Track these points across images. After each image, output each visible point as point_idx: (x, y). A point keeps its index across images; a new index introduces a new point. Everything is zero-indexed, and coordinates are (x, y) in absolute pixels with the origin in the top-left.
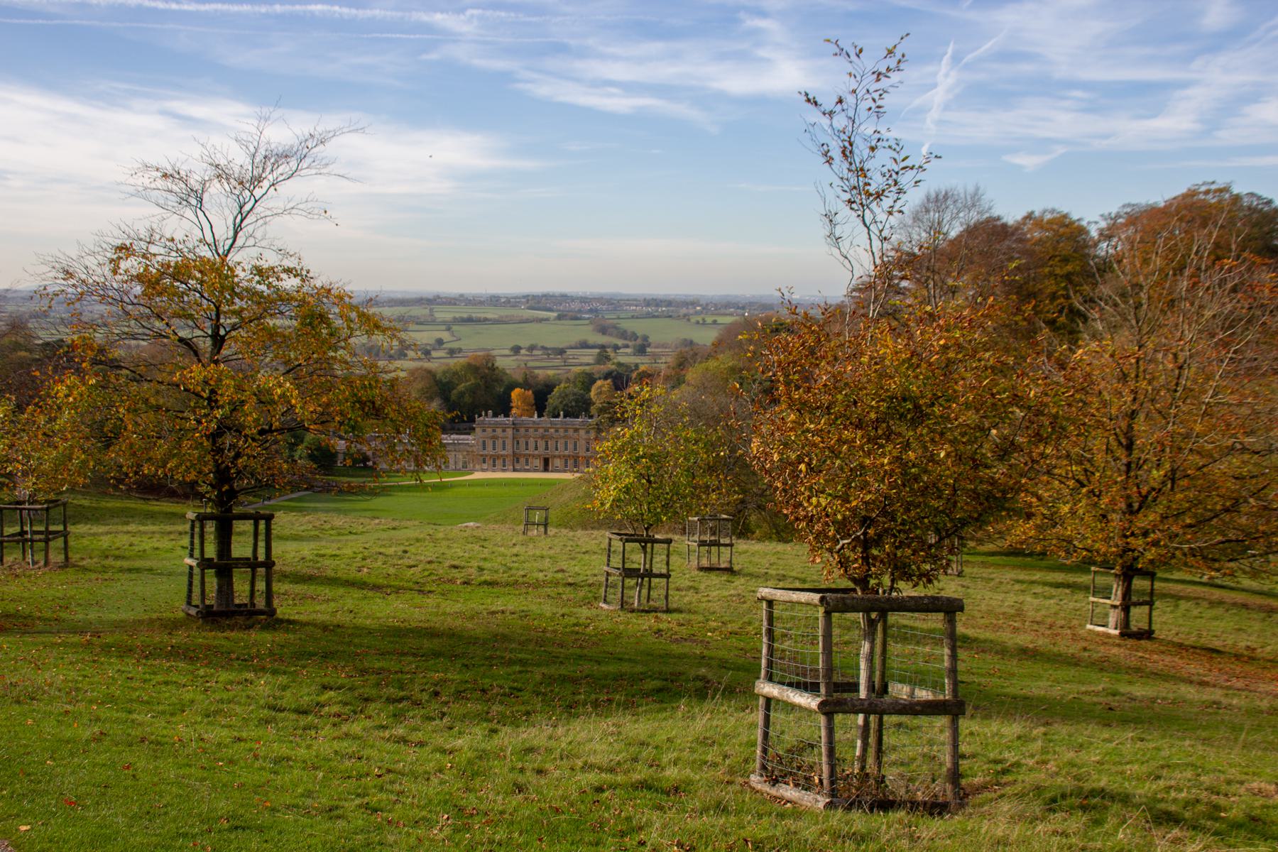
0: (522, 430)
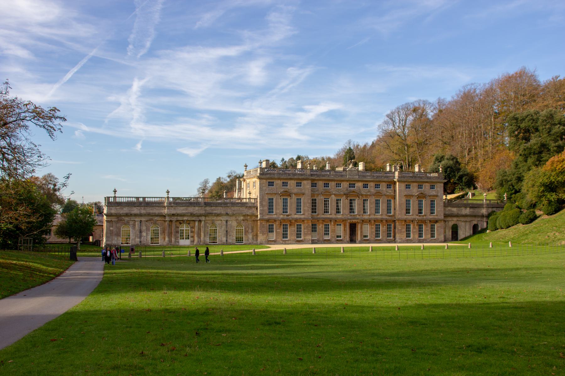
0: (320, 184)
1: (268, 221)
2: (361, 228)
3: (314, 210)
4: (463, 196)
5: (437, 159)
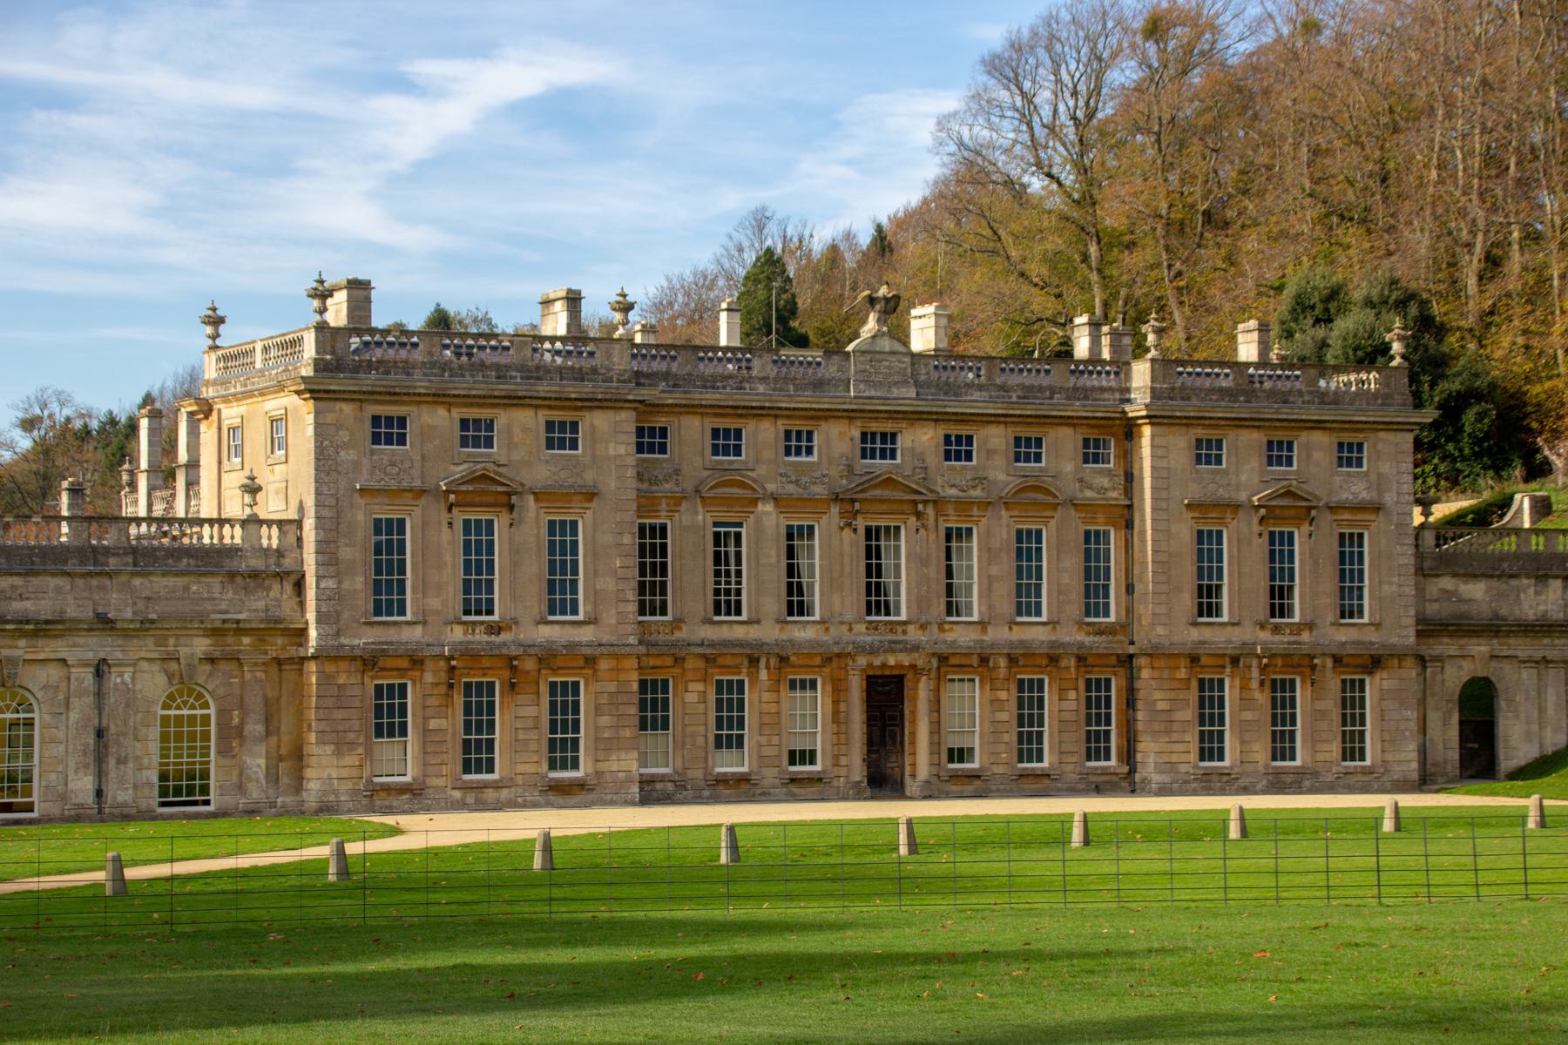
0: (691, 434)
1: (369, 661)
2: (936, 705)
3: (652, 591)
4: (1481, 518)
5: (1301, 306)
